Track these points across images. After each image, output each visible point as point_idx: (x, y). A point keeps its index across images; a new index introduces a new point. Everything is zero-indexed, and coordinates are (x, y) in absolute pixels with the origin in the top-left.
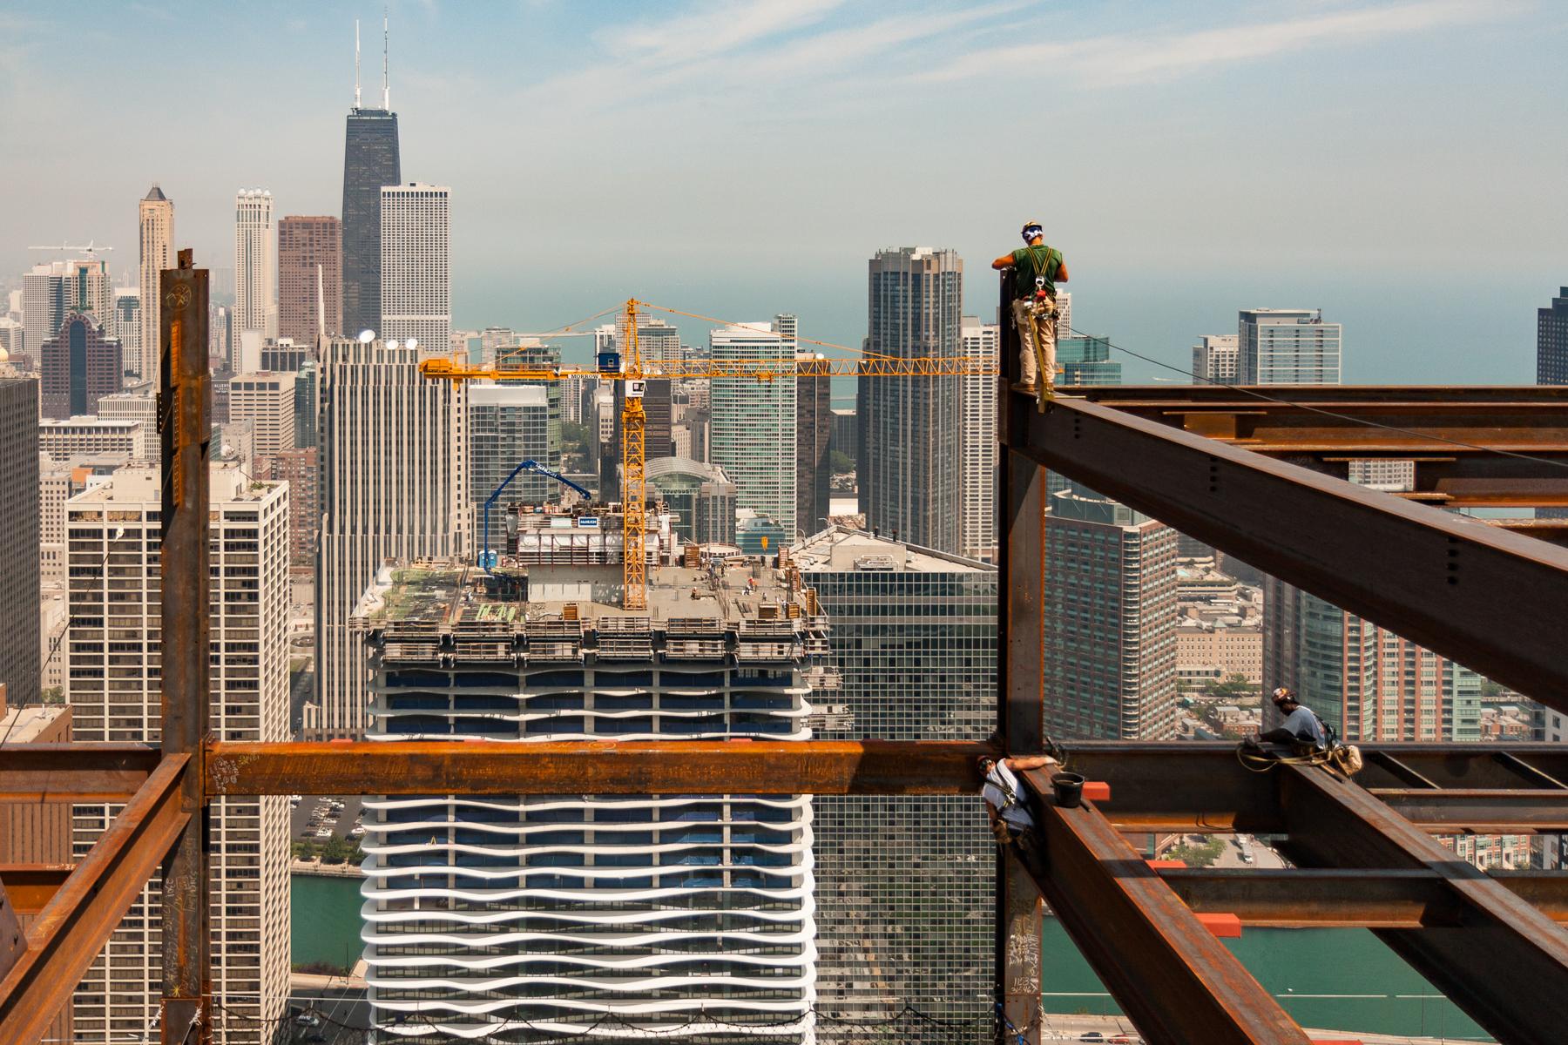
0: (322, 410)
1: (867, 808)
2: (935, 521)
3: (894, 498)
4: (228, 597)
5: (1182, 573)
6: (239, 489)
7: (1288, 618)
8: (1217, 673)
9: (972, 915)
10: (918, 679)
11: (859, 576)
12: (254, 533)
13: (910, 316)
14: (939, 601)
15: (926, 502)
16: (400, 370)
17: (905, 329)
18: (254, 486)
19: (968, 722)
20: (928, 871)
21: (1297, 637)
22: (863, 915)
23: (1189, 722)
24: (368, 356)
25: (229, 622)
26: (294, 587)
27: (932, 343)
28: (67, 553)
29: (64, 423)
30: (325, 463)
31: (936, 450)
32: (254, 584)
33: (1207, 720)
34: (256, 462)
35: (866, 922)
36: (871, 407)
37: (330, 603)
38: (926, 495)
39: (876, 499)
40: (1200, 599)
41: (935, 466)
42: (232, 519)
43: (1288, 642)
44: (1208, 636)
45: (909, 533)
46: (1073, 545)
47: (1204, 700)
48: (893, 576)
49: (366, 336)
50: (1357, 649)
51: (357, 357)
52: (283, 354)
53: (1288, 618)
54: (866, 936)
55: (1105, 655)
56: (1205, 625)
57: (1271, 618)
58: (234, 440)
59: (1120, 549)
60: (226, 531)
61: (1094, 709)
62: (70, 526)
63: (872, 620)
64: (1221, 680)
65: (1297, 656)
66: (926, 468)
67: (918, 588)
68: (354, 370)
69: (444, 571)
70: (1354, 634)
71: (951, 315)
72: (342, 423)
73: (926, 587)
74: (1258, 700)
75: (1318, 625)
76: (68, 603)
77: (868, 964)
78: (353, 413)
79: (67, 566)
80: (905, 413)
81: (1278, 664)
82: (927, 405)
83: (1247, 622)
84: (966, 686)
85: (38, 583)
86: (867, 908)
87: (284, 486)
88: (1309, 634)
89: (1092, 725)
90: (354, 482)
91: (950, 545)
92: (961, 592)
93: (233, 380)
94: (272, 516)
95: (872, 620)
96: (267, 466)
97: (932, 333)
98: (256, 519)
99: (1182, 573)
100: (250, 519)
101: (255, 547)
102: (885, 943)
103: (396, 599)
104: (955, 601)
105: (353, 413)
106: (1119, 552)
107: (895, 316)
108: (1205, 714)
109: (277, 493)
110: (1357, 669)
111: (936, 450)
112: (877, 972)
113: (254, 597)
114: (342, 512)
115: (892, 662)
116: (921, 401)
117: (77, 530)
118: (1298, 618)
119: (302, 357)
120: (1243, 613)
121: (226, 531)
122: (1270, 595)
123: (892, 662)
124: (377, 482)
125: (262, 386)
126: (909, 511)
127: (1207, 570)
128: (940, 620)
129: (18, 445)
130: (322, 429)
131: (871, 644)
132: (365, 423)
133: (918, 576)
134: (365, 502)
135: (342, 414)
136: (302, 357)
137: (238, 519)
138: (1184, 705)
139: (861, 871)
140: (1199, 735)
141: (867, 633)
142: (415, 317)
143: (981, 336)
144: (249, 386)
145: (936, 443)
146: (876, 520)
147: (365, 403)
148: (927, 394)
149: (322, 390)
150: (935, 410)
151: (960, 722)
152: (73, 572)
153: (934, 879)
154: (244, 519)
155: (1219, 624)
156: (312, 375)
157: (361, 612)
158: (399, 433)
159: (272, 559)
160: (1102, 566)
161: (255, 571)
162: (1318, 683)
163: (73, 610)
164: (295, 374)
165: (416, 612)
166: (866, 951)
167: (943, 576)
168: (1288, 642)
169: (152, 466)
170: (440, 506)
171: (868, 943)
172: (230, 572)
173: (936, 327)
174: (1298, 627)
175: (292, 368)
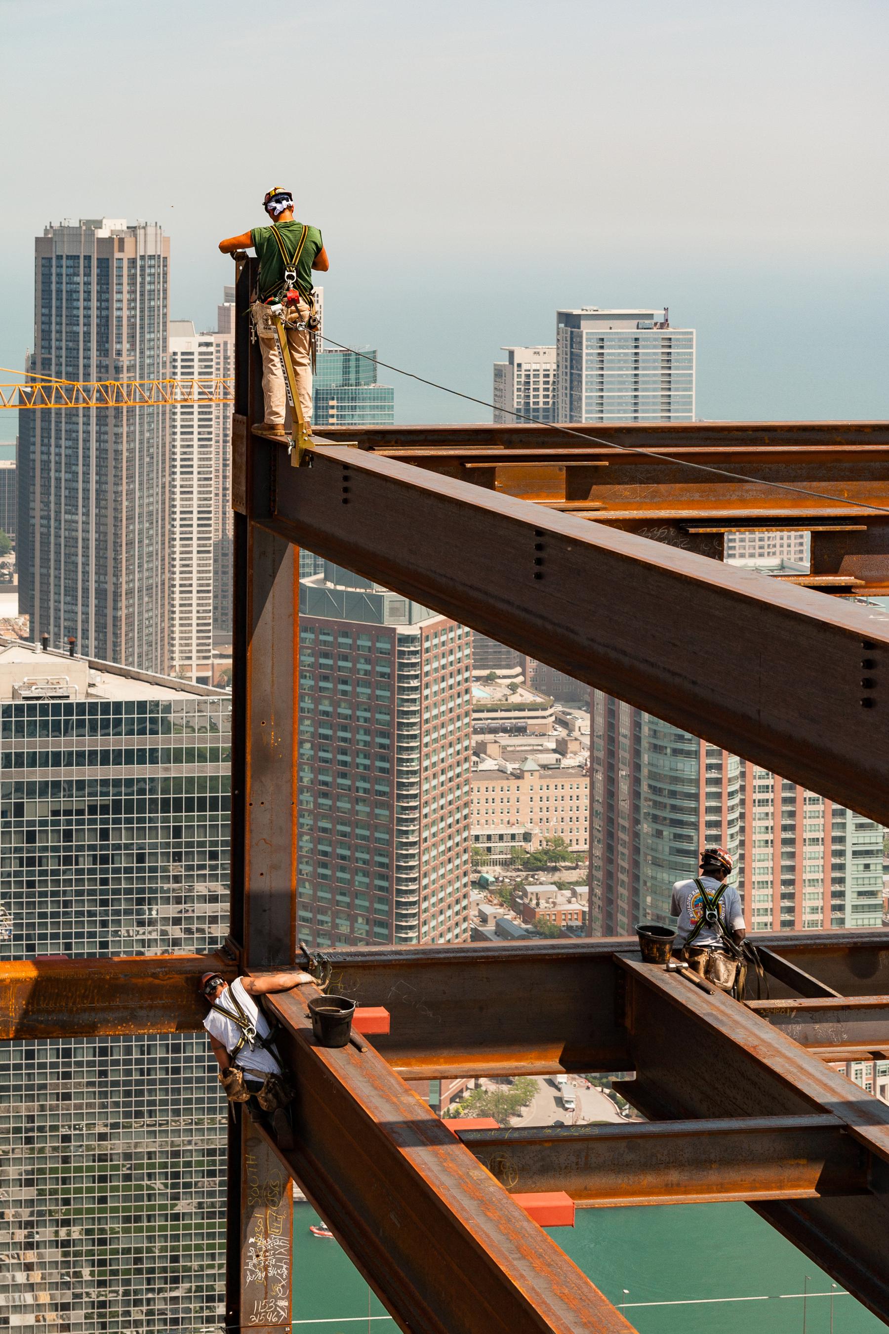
1: (30, 1055)
2: (130, 625)
3: (71, 591)
5: (480, 693)
7: (624, 754)
8: (527, 837)
9: (183, 1206)
10: (104, 860)
11: (19, 709)
13: (94, 321)
14: (136, 742)
15: (116, 595)
17: (87, 341)
19: (177, 921)
20: (117, 1146)
21: (636, 781)
22: (25, 1214)
23: (488, 909)
27: (125, 360)
31: (130, 518)
33: (513, 905)
35: (29, 1224)
36: (38, 457)
38: (117, 585)
39: (45, 593)
40: (505, 730)
41: (130, 543)
43: (624, 787)
44: (514, 783)
45: (92, 643)
46: (326, 655)
47: (508, 876)
48: (69, 708)
50: (718, 796)
53: (624, 754)
54: (29, 1246)
55: (371, 814)
56: (510, 767)
57: (601, 754)
59: (393, 662)
61: (356, 895)
63: (38, 775)
64: (533, 847)
65: (636, 808)
66: (117, 545)
67: (105, 724)
70: (713, 774)
71: (152, 317)
73: (118, 722)
74: (582, 873)
75: (666, 763)
77: (31, 1287)
80: (87, 465)
81: (610, 821)
82: (118, 452)
83: (569, 761)
84: (175, 869)
86: (30, 1203)
88: (653, 776)
89: (352, 919)
91: (153, 659)
92: (167, 731)
95: (38, 775)
97: (126, 346)
99: (480, 693)
102: (54, 1254)
104: (160, 742)
106: (391, 664)
107: (73, 320)
108: (511, 898)
110: (717, 824)
111: (130, 518)
112: (44, 1297)
115: (68, 835)
116: (110, 446)
118: (637, 753)
120: (561, 749)
122: (600, 721)
123: (68, 835)
126: (92, 610)
127: (513, 688)
128: (137, 771)
131: (37, 809)
133: (106, 707)
138: (481, 884)
139: (21, 1150)
140: (501, 931)
141: (31, 793)
143: (196, 350)
145: (131, 509)
146: (45, 625)
148: (118, 435)
150: (130, 460)
151: (165, 920)
153: (128, 1156)
155: (530, 765)
160: (367, 684)
162: (665, 846)
166: (29, 1267)
167: (142, 705)
168: (624, 787)
171: (31, 1256)
173: (132, 336)
174: (637, 767)
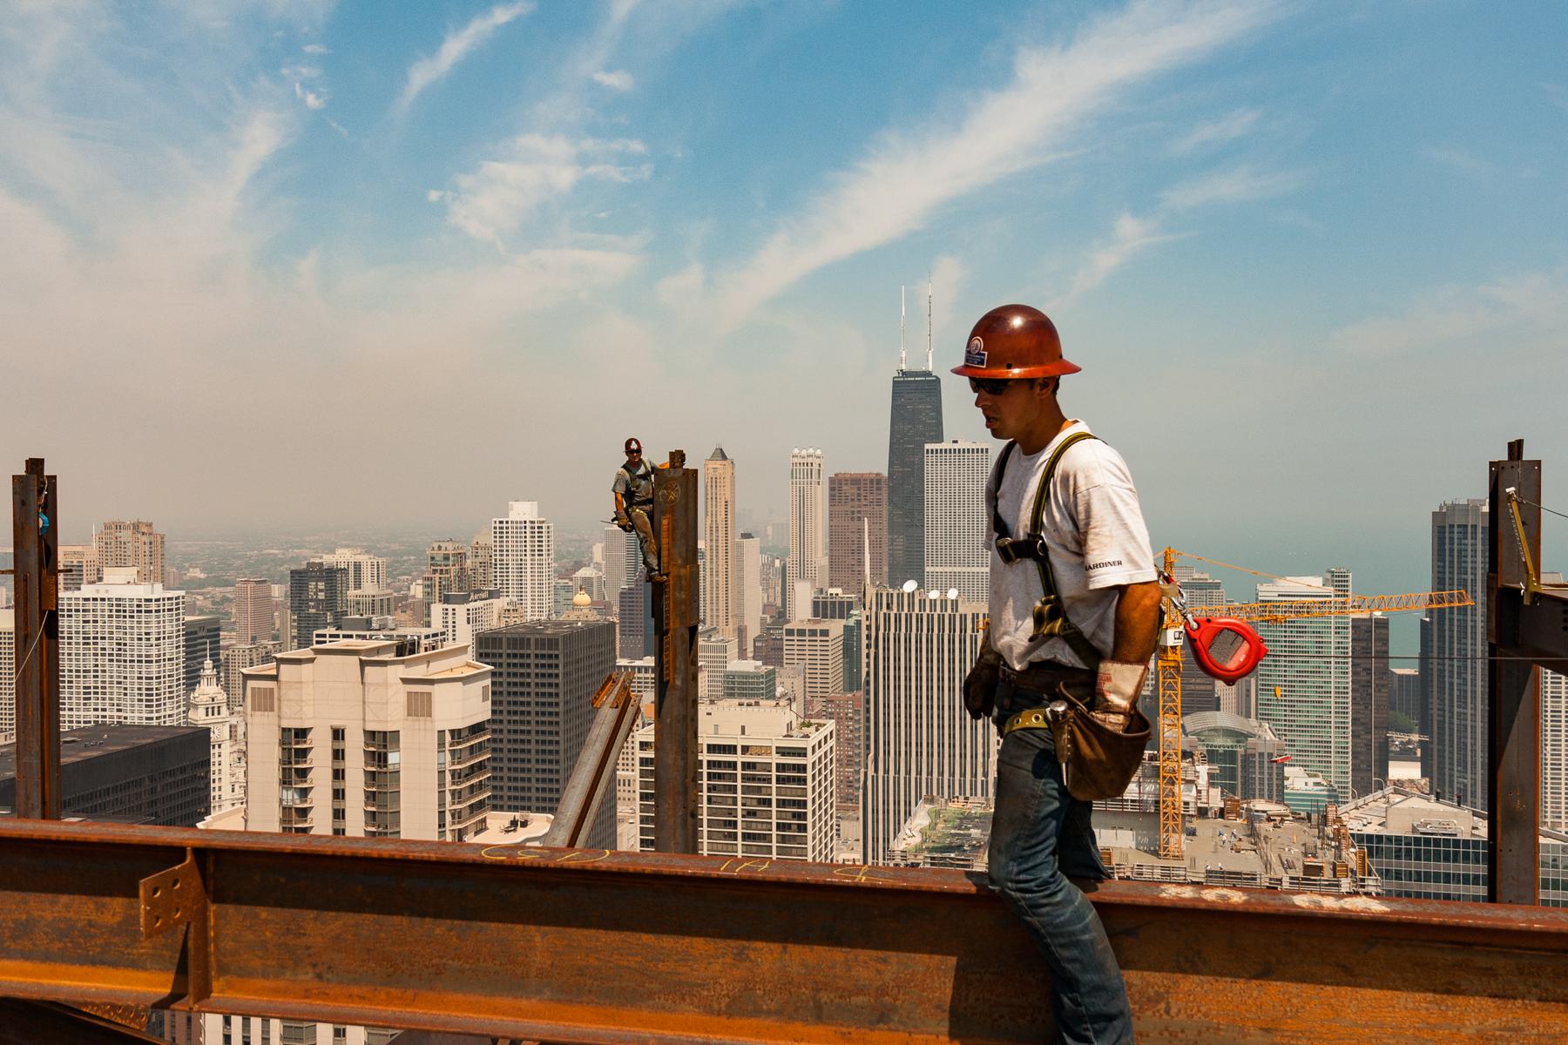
0: (868, 656)
4: (780, 827)
6: (789, 726)
12: (803, 768)
16: (941, 618)
18: (804, 725)
24: (911, 605)
26: (842, 823)
28: (638, 779)
29: (638, 663)
30: (869, 708)
32: (803, 816)
34: (807, 704)
37: (875, 840)
49: (910, 586)
51: (900, 606)
52: (833, 603)
58: (788, 682)
62: (639, 754)
68: (898, 618)
69: (979, 811)
72: (886, 669)
76: (638, 825)
78: (897, 659)
79: (638, 791)
85: (614, 807)
87: (831, 725)
90: (897, 725)
93: (786, 627)
94: (820, 753)
96: (818, 707)
101: (804, 781)
103: (934, 835)
105: (897, 659)
109: (824, 731)
113: (803, 828)
114: (887, 753)
119: (850, 605)
124: (919, 726)
125: (813, 633)
130: (868, 674)
132: (908, 669)
134: (908, 744)
135: (886, 659)
136: (850, 605)
137: (789, 754)
142: (957, 569)
144: (801, 632)
147: (908, 650)
149: (868, 637)
154: (794, 755)
156: (859, 623)
157: (898, 845)
158: (941, 679)
159: (818, 793)
161: (804, 804)
164: (844, 622)
165: (949, 849)
169: (712, 702)
170: (980, 751)
175: (841, 617)
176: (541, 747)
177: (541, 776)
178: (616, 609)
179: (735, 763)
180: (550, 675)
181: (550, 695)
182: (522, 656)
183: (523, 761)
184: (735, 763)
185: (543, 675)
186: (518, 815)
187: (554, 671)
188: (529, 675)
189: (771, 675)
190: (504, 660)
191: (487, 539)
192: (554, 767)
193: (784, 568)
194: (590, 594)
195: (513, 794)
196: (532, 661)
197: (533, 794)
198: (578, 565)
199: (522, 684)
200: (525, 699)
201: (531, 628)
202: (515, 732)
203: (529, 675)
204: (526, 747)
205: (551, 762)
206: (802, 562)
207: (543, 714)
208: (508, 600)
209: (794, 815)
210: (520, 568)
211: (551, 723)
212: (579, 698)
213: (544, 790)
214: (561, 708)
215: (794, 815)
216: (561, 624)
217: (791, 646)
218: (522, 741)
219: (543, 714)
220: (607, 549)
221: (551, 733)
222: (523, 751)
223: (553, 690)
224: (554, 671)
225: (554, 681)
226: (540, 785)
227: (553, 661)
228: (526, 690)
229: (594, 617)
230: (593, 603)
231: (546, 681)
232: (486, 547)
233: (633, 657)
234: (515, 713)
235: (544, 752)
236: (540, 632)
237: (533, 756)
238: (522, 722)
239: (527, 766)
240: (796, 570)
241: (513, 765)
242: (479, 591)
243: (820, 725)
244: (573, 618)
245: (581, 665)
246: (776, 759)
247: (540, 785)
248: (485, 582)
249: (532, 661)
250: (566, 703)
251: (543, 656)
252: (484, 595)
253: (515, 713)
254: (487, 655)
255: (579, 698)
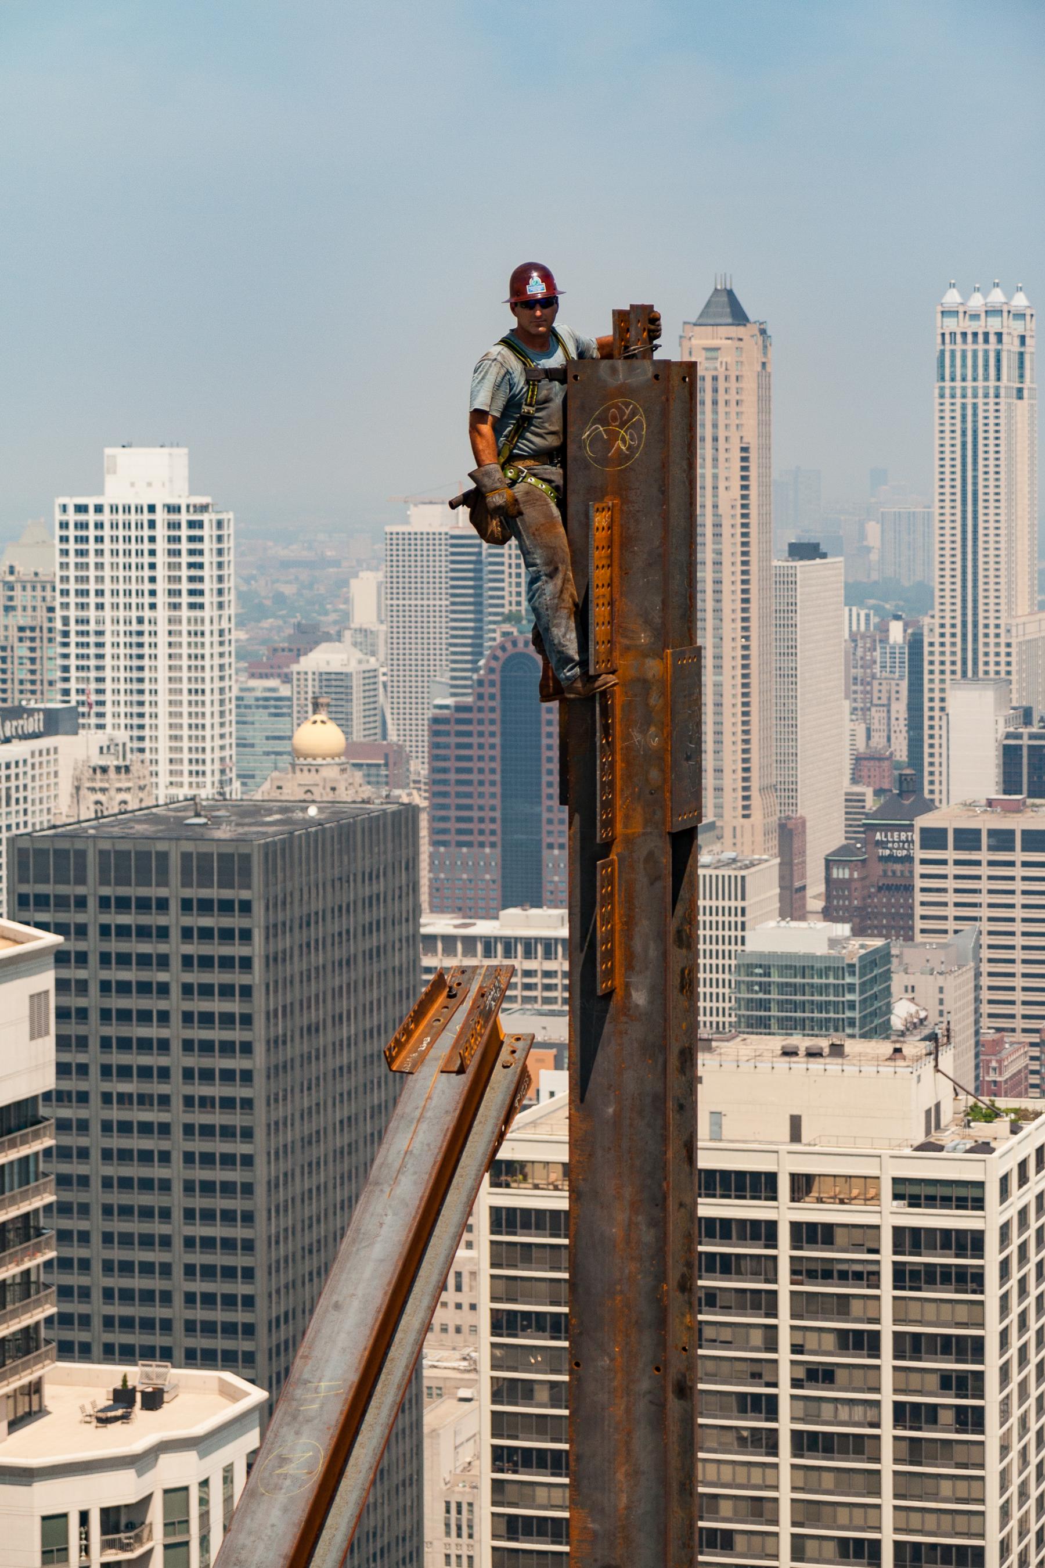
4: (903, 1414)
6: (933, 1117)
12: (974, 1242)
18: (974, 1114)
25: (905, 1486)
28: (486, 1271)
34: (984, 1052)
42: (915, 1201)
60: (898, 1232)
79: (486, 1306)
98: (978, 1204)
100: (962, 1203)
101: (976, 1280)
113: (972, 1420)
117: (511, 1211)
121: (898, 1231)
129: (367, 983)
137: (931, 1201)
152: (501, 1323)
154: (946, 1202)
161: (976, 1348)
163: (500, 1424)
172: (909, 1346)
176: (201, 1174)
177: (198, 1258)
178: (419, 767)
179: (772, 1225)
180: (227, 963)
181: (227, 1019)
182: (144, 905)
183: (146, 1213)
184: (772, 1225)
185: (206, 962)
186: (136, 1374)
187: (236, 950)
188: (163, 961)
189: (877, 965)
190: (91, 917)
191: (42, 557)
192: (239, 1232)
193: (915, 645)
194: (344, 722)
195: (117, 1310)
196: (174, 919)
197: (178, 1312)
198: (308, 637)
199: (144, 988)
200: (153, 1031)
201: (172, 823)
202: (125, 1127)
203: (163, 961)
204: (157, 1172)
205: (228, 1216)
206: (969, 629)
207: (207, 1075)
208: (100, 738)
209: (947, 1382)
210: (137, 643)
211: (228, 1103)
212: (313, 1030)
213: (209, 1299)
214: (258, 1061)
215: (947, 1382)
216: (251, 812)
217: (936, 882)
218: (146, 1156)
219: (207, 1075)
220: (394, 588)
221: (227, 1132)
222: (146, 1184)
223: (234, 1006)
224: (236, 950)
225: (237, 978)
226: (199, 1286)
227: (235, 921)
228: (154, 1004)
229: (353, 790)
230: (351, 749)
231: (216, 977)
232: (37, 583)
233: (469, 911)
234: (125, 1072)
235: (208, 1187)
236: (196, 835)
237: (177, 1200)
238: (144, 1100)
239: (158, 1228)
240: (952, 652)
241: (119, 1226)
242: (18, 712)
243: (1023, 1116)
244: (292, 792)
245: (317, 932)
246: (892, 1215)
247: (199, 1286)
248: (34, 685)
249: (174, 919)
250: (274, 1043)
251: (206, 906)
252: (31, 724)
253: (125, 1072)
254: (42, 901)
255: (313, 1030)
